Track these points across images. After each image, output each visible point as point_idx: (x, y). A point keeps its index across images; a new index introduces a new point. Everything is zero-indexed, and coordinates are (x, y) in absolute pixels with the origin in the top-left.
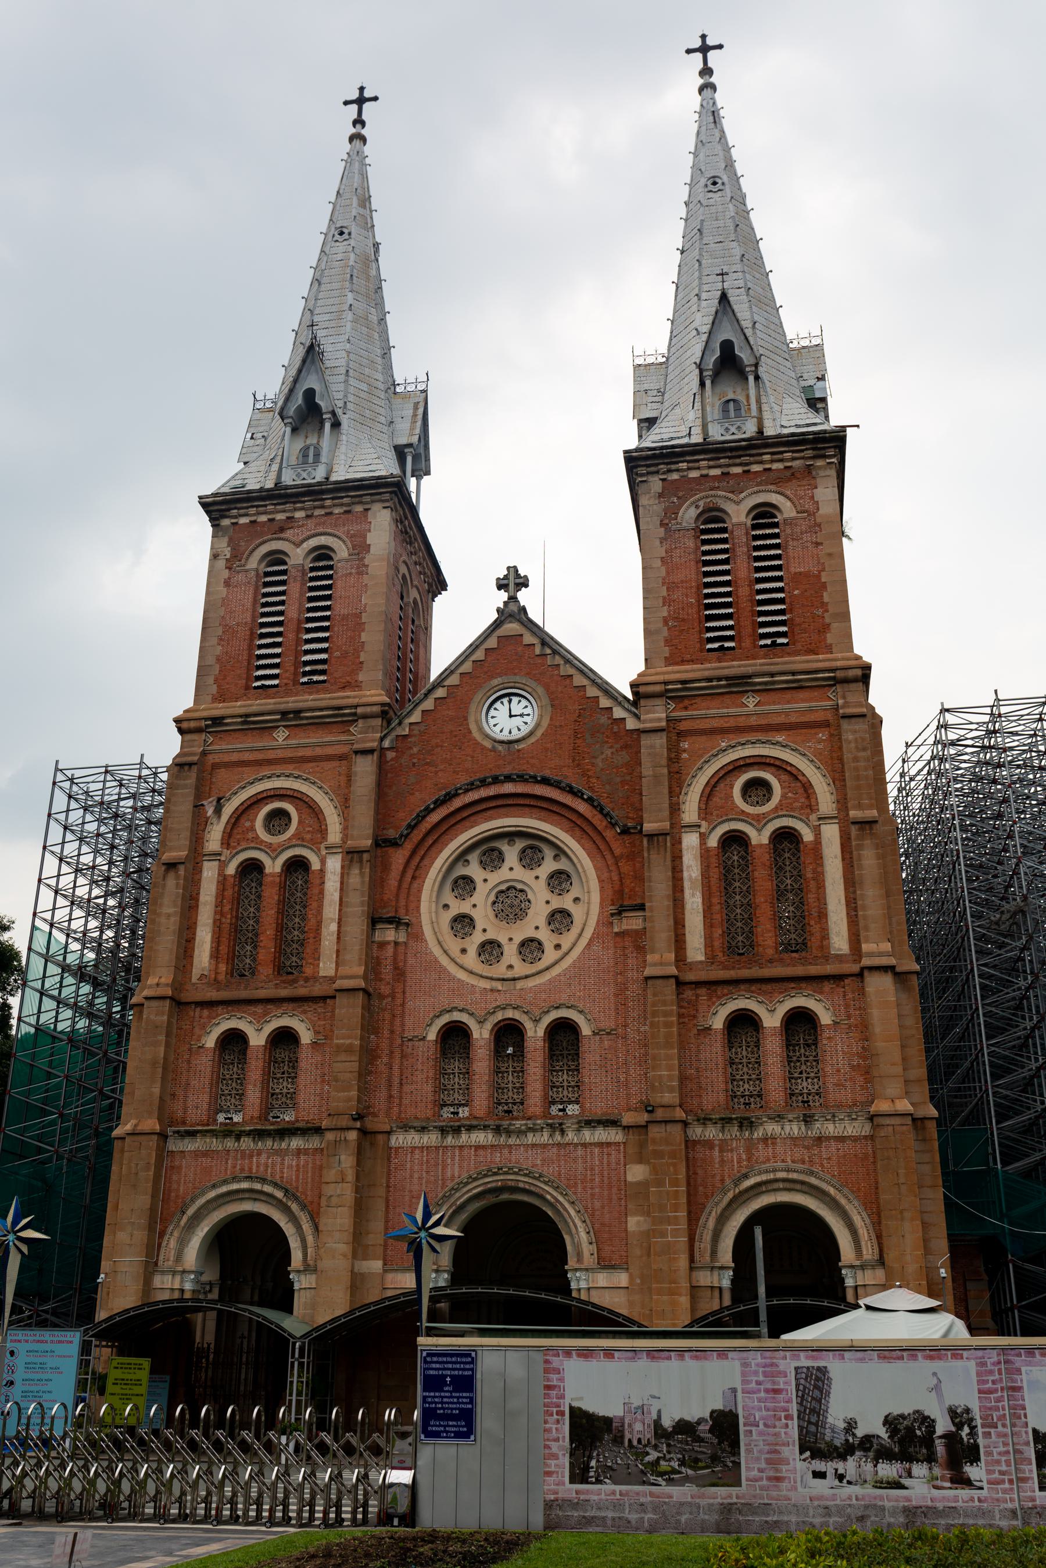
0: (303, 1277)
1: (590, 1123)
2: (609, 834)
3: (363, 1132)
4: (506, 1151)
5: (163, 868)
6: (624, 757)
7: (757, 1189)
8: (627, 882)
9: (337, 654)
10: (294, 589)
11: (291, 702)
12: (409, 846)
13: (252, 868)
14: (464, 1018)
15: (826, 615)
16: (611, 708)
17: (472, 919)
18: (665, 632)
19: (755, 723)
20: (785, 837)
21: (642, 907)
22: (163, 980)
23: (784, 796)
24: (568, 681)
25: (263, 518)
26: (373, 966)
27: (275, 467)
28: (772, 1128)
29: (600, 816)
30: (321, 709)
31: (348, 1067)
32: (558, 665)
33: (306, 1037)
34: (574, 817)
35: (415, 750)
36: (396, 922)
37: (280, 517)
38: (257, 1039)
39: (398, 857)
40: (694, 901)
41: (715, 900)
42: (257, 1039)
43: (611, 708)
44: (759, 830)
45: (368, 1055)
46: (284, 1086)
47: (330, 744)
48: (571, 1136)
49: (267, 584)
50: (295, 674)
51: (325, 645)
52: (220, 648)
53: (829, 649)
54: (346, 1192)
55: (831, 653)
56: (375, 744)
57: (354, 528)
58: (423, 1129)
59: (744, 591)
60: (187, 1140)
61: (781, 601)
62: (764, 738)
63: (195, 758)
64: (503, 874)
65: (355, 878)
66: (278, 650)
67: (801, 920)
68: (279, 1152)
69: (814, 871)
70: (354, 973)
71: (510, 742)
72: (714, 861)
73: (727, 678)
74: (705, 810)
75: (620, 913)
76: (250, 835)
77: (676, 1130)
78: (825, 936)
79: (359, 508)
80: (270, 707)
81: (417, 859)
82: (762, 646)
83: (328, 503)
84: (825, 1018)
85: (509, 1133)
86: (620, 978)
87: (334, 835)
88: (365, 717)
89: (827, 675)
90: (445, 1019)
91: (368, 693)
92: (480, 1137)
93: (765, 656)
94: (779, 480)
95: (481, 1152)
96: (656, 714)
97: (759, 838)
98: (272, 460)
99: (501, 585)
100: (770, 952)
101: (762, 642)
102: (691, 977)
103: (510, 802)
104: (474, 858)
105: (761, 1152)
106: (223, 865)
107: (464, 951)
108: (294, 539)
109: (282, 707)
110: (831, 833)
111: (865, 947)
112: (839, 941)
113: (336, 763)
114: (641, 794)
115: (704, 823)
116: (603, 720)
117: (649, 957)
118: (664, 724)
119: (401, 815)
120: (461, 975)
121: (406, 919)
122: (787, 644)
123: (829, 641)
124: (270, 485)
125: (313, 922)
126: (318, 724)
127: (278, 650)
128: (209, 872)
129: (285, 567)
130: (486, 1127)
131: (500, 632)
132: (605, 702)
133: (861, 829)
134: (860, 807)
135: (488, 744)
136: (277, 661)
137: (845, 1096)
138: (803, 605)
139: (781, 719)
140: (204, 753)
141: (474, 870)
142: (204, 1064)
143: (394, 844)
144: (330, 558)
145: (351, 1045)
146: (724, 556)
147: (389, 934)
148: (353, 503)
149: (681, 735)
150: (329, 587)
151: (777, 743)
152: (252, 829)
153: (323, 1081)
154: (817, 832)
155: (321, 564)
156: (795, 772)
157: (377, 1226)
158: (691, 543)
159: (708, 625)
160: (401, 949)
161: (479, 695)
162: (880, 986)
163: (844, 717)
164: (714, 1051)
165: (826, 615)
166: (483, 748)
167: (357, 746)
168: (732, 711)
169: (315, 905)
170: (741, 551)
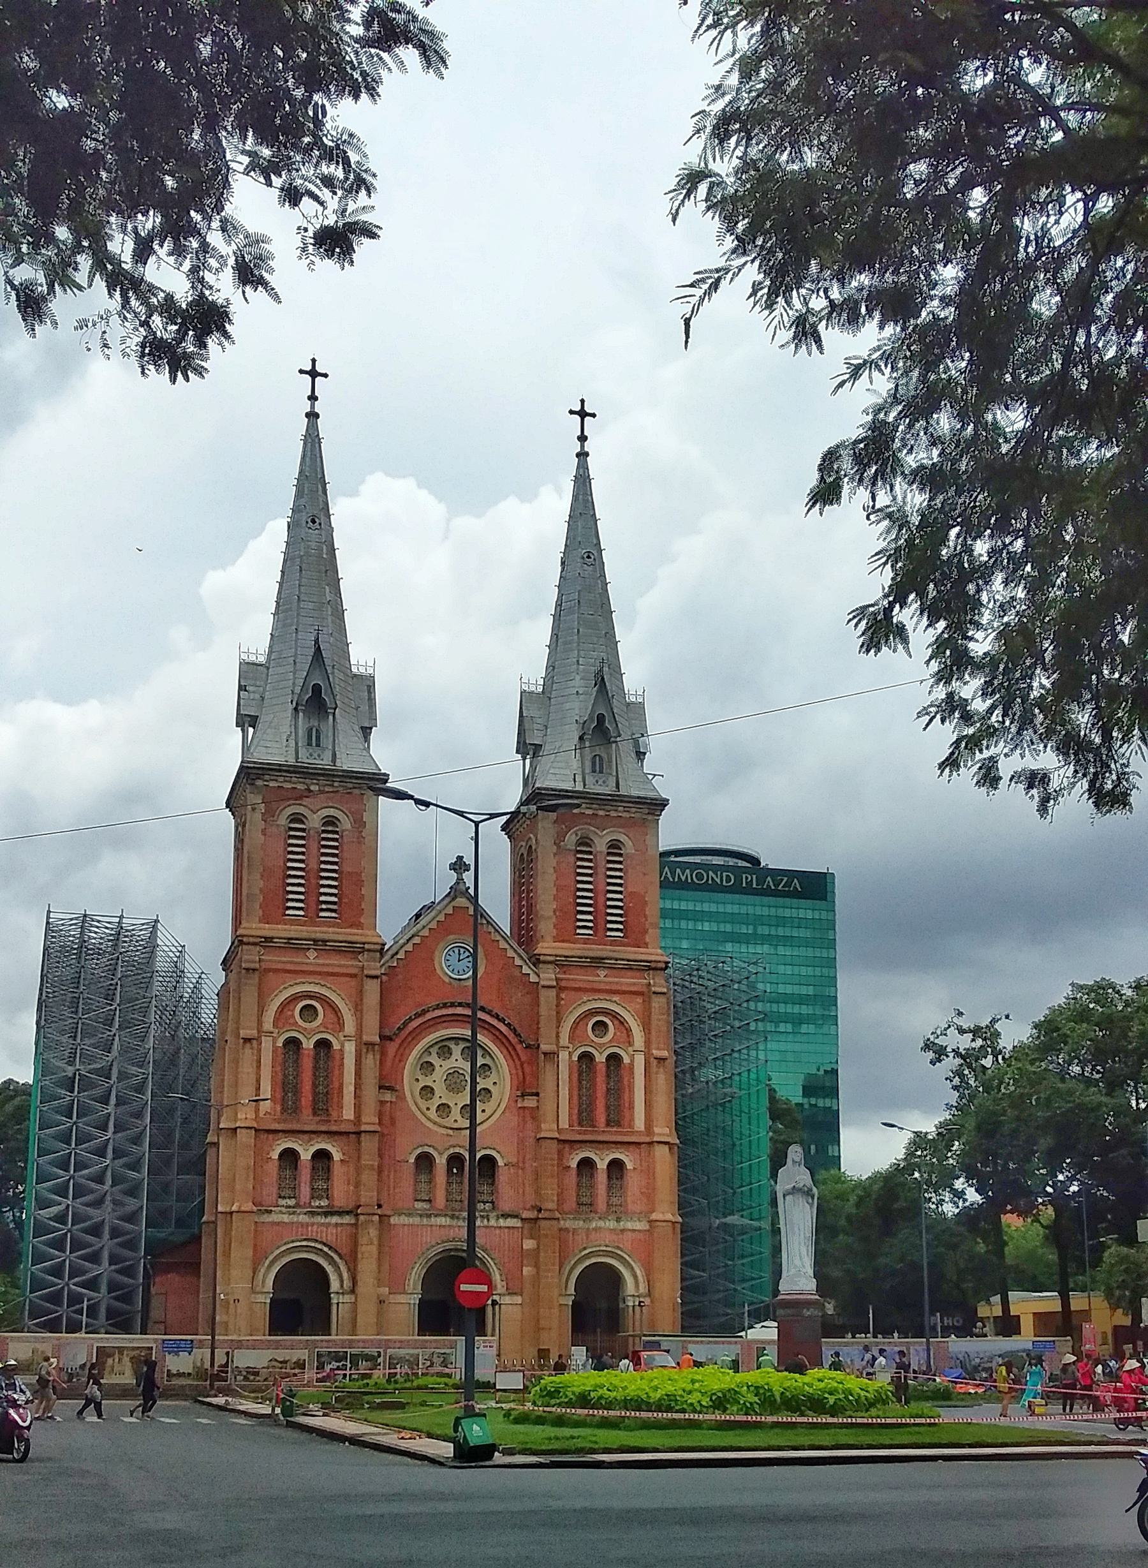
0: (341, 1296)
1: (505, 1216)
2: (518, 1047)
3: (380, 1216)
4: (457, 1229)
5: (242, 1041)
6: (527, 999)
7: (587, 1256)
8: (528, 1078)
9: (346, 900)
10: (314, 846)
11: (319, 932)
12: (398, 1041)
13: (293, 1044)
14: (431, 1150)
16: (521, 966)
17: (433, 1089)
18: (554, 920)
20: (614, 1059)
21: (537, 1094)
22: (248, 1116)
23: (615, 1034)
24: (496, 944)
25: (289, 786)
26: (380, 1115)
27: (292, 743)
28: (601, 1224)
29: (513, 1035)
30: (341, 942)
31: (369, 1178)
32: (490, 933)
33: (337, 1156)
34: (497, 1033)
35: (400, 977)
36: (391, 1089)
37: (300, 787)
38: (306, 1155)
39: (392, 1048)
40: (564, 1092)
41: (575, 1093)
42: (306, 1155)
43: (521, 966)
44: (601, 1053)
45: (380, 1171)
46: (321, 1184)
47: (347, 966)
48: (493, 1222)
49: (291, 837)
50: (317, 909)
51: (335, 891)
52: (262, 882)
53: (646, 945)
54: (374, 1249)
56: (378, 973)
57: (354, 807)
58: (410, 1215)
59: (601, 900)
60: (266, 1215)
63: (257, 966)
64: (450, 1063)
65: (370, 1061)
66: (302, 889)
67: (619, 1109)
68: (328, 1225)
69: (629, 1081)
70: (370, 1120)
71: (460, 980)
72: (575, 1070)
73: (590, 958)
74: (571, 1039)
75: (523, 1095)
76: (291, 1021)
77: (554, 1222)
78: (632, 1120)
79: (357, 791)
80: (304, 935)
81: (402, 1049)
83: (336, 784)
84: (629, 1166)
85: (458, 1218)
86: (521, 1134)
87: (350, 1027)
88: (369, 950)
90: (419, 1151)
91: (369, 933)
92: (442, 1221)
94: (627, 824)
95: (442, 1229)
96: (548, 976)
97: (600, 1058)
98: (289, 736)
99: (453, 867)
100: (603, 1125)
102: (562, 1138)
103: (460, 1018)
104: (434, 1050)
105: (593, 1236)
106: (275, 1040)
107: (428, 1109)
108: (312, 807)
109: (313, 936)
110: (640, 1060)
111: (656, 1130)
112: (639, 1123)
113: (348, 979)
114: (538, 1023)
115: (571, 1046)
116: (517, 973)
117: (542, 1125)
118: (555, 983)
119: (392, 1020)
120: (429, 1124)
121: (398, 1087)
124: (292, 761)
125: (336, 1085)
126: (338, 951)
127: (302, 889)
128: (266, 1043)
129: (304, 827)
130: (446, 1215)
131: (456, 903)
132: (518, 962)
133: (659, 1063)
134: (658, 1049)
135: (447, 980)
136: (302, 897)
137: (637, 1208)
140: (260, 960)
141: (434, 1059)
142: (273, 1168)
143: (390, 1039)
144: (333, 824)
145: (372, 1165)
146: (590, 871)
147: (388, 1096)
148: (355, 788)
149: (561, 989)
150: (336, 848)
152: (293, 1016)
153: (348, 1184)
154: (632, 1057)
155: (330, 828)
156: (622, 1020)
157: (386, 1267)
158: (572, 859)
159: (579, 917)
160: (393, 1105)
161: (441, 945)
162: (662, 1152)
163: (654, 993)
164: (571, 1179)
166: (444, 981)
167: (366, 972)
168: (590, 978)
169: (336, 1072)
170: (601, 870)
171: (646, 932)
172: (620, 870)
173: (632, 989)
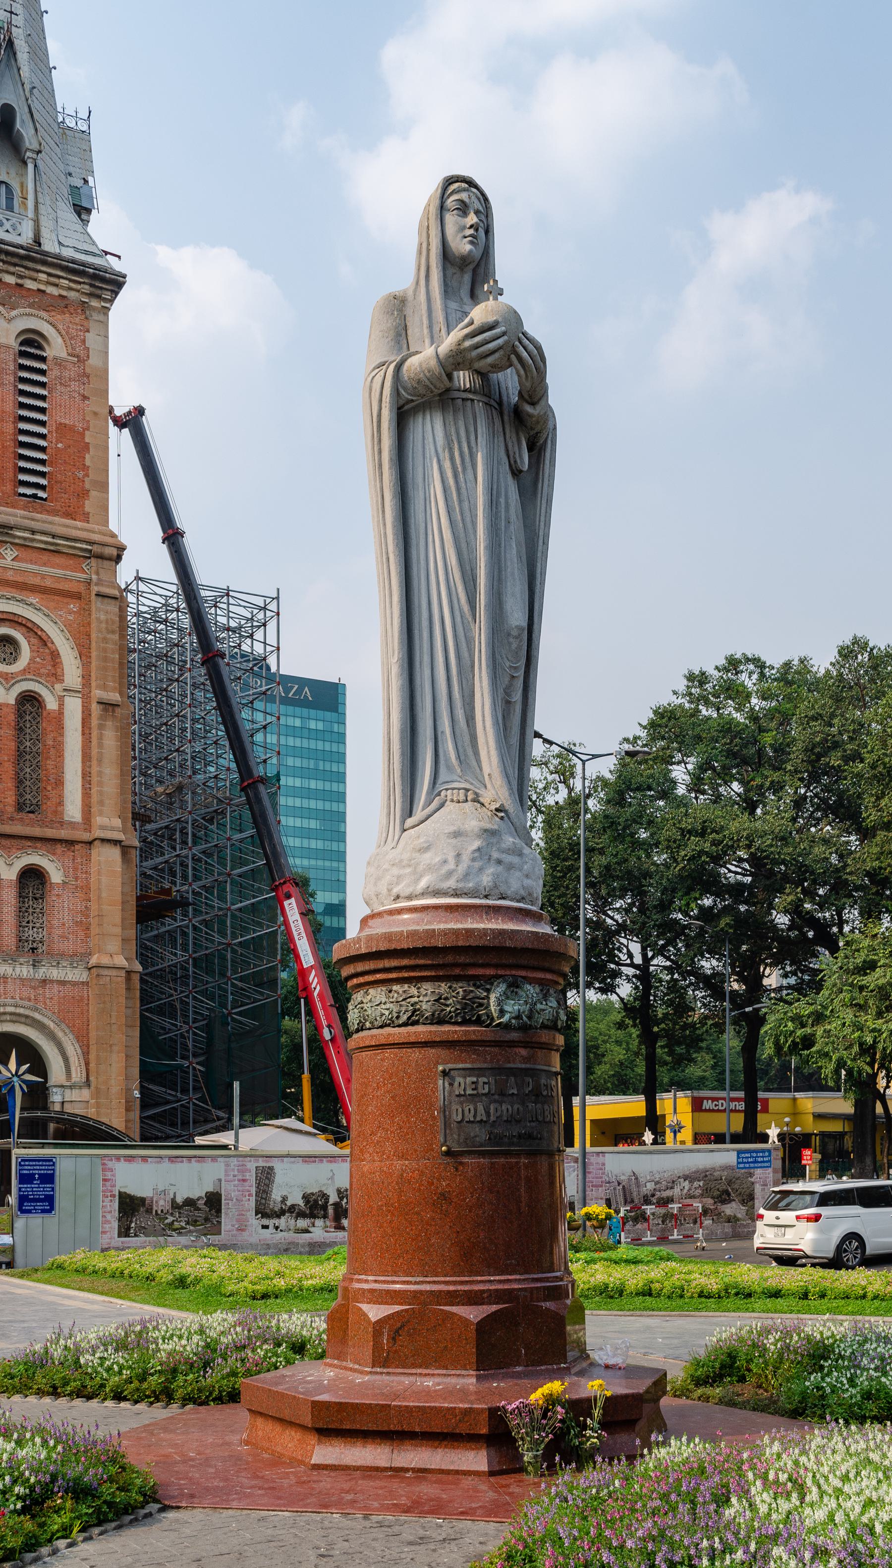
15: (86, 479)
19: (11, 578)
53: (86, 518)
55: (88, 522)
61: (43, 449)
62: (19, 597)
82: (20, 495)
89: (84, 546)
93: (25, 508)
101: (22, 490)
122: (45, 500)
123: (87, 509)
138: (65, 462)
139: (37, 581)
151: (31, 605)
165: (86, 479)
171: (84, 494)
172: (43, 385)
173: (66, 586)
